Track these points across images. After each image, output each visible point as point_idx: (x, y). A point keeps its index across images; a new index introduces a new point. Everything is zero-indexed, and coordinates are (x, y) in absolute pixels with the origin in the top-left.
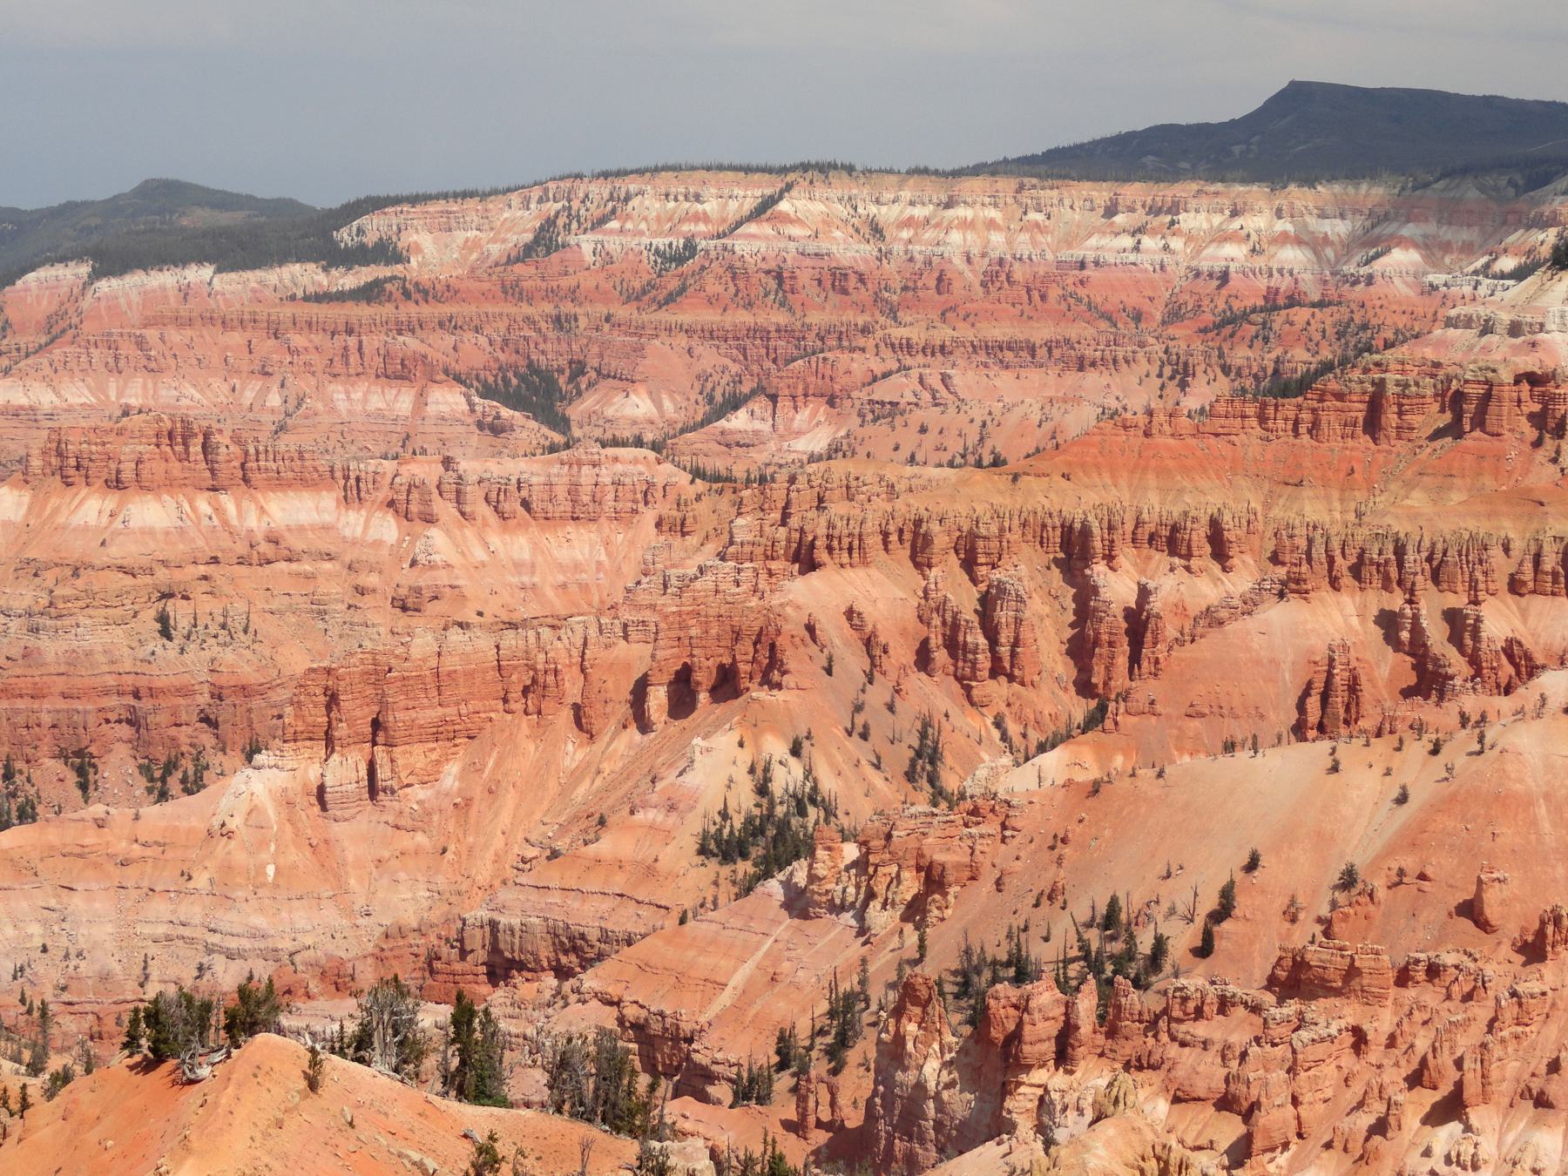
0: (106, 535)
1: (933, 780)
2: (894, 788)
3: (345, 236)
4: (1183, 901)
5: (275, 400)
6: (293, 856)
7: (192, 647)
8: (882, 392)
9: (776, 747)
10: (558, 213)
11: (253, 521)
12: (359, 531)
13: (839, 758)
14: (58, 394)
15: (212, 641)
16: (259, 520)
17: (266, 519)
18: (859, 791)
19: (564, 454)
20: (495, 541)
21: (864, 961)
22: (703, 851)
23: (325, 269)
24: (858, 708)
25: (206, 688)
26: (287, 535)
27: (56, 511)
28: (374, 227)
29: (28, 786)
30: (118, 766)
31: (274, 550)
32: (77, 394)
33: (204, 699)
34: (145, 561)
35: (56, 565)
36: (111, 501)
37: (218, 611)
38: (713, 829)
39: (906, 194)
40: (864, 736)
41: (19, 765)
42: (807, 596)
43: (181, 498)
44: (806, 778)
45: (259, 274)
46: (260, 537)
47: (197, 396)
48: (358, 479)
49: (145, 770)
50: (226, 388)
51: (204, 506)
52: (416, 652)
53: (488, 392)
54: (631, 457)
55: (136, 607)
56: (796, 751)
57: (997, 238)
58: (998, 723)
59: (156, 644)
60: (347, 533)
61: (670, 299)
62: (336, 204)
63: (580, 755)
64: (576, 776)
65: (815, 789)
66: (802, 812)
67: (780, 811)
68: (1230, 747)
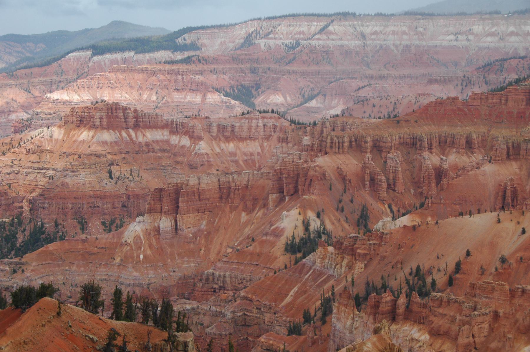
0: (90, 144)
1: (365, 226)
2: (352, 228)
6: (149, 252)
7: (120, 182)
9: (311, 215)
11: (140, 139)
12: (177, 142)
13: (333, 218)
15: (126, 180)
16: (143, 139)
17: (145, 138)
18: (340, 229)
19: (247, 116)
20: (223, 145)
21: (333, 287)
22: (286, 250)
24: (340, 201)
25: (124, 196)
26: (152, 143)
27: (74, 136)
29: (63, 229)
35: (73, 154)
36: (92, 133)
37: (128, 169)
38: (289, 242)
40: (342, 210)
41: (60, 222)
42: (324, 162)
43: (116, 131)
44: (321, 225)
46: (143, 144)
48: (177, 125)
49: (103, 223)
51: (124, 134)
52: (191, 183)
54: (269, 117)
55: (101, 168)
56: (318, 216)
58: (390, 207)
59: (107, 181)
60: (173, 142)
63: (246, 218)
65: (324, 229)
66: (320, 237)
67: (312, 236)
68: (461, 214)
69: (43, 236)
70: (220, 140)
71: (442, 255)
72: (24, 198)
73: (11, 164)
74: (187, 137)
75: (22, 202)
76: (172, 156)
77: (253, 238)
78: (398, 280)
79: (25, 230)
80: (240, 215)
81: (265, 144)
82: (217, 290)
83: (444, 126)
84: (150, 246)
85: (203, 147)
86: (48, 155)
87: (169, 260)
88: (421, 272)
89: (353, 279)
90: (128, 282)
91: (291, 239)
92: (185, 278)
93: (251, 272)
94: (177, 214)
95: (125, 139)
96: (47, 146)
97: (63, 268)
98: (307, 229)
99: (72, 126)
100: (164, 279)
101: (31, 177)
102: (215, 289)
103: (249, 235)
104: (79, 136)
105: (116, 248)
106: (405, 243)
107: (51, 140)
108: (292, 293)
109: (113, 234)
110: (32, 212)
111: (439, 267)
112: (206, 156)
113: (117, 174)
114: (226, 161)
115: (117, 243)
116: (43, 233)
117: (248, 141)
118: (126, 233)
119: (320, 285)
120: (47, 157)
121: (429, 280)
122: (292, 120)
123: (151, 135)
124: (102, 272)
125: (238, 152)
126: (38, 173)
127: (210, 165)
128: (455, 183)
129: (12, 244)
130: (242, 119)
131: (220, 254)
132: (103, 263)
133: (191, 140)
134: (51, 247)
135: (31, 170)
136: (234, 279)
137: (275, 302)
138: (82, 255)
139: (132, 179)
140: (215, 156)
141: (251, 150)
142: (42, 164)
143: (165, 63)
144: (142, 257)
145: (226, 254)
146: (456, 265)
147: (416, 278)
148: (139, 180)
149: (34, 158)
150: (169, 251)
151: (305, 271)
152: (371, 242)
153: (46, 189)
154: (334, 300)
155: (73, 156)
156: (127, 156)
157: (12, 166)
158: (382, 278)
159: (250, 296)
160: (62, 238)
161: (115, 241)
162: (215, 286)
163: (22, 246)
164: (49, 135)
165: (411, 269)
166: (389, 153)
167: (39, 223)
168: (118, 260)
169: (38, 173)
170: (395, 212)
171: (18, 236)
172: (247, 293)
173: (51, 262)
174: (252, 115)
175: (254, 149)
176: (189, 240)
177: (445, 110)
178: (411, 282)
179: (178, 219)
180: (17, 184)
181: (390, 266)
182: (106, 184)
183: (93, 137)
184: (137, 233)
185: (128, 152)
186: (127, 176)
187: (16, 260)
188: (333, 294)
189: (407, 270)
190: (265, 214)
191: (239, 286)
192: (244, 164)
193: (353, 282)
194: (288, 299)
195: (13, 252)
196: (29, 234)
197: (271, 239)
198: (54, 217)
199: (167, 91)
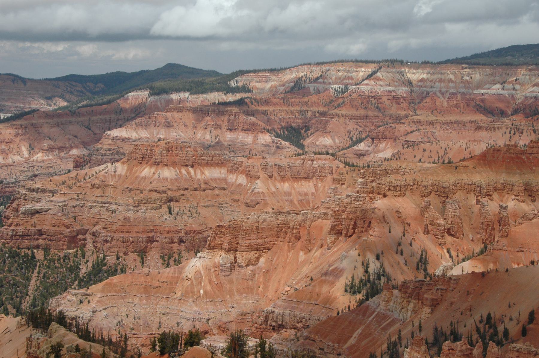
0: (151, 180)
1: (425, 270)
2: (411, 272)
3: (232, 83)
4: (515, 315)
5: (208, 137)
6: (209, 288)
7: (179, 218)
8: (410, 138)
10: (302, 77)
11: (199, 176)
12: (234, 180)
13: (392, 260)
14: (137, 134)
15: (184, 216)
17: (203, 176)
19: (302, 157)
20: (278, 185)
21: (400, 331)
22: (346, 291)
23: (225, 94)
26: (211, 181)
28: (241, 81)
29: (124, 261)
30: (153, 256)
31: (206, 187)
32: (144, 134)
33: (182, 234)
34: (164, 189)
36: (153, 170)
37: (187, 205)
38: (349, 283)
39: (420, 71)
40: (402, 254)
41: (121, 254)
44: (381, 267)
45: (205, 96)
47: (183, 135)
49: (162, 257)
50: (192, 133)
53: (278, 136)
54: (323, 158)
55: (161, 204)
56: (378, 258)
57: (451, 85)
60: (230, 181)
61: (339, 106)
62: (229, 72)
63: (304, 257)
64: (304, 263)
65: (384, 271)
66: (380, 279)
67: (372, 278)
69: (105, 268)
70: (275, 179)
71: (514, 304)
72: (87, 230)
73: (77, 197)
74: (244, 176)
75: (85, 234)
76: (229, 194)
77: (312, 278)
78: (468, 327)
79: (88, 261)
80: (298, 254)
81: (319, 185)
82: (276, 328)
83: (502, 173)
84: (210, 282)
85: (259, 185)
86: (112, 190)
87: (228, 296)
88: (493, 321)
89: (420, 324)
90: (188, 316)
91: (351, 280)
92: (244, 314)
93: (310, 312)
94: (237, 250)
95: (184, 176)
96: (110, 181)
97: (127, 300)
98: (366, 271)
99: (135, 162)
100: (223, 314)
101: (95, 210)
102: (274, 326)
103: (307, 274)
104: (141, 172)
105: (177, 283)
106: (474, 290)
107: (115, 176)
108: (355, 335)
109: (174, 268)
110: (95, 244)
111: (511, 317)
112: (261, 195)
113: (176, 210)
114: (282, 200)
115: (178, 277)
116: (105, 265)
117: (303, 181)
118: (187, 268)
119: (385, 329)
120: (110, 192)
121: (501, 328)
122: (347, 163)
123: (210, 173)
124: (163, 305)
125: (293, 191)
126: (102, 207)
127: (266, 204)
128: (518, 230)
129: (75, 274)
130: (297, 159)
131: (278, 292)
132: (165, 297)
133: (247, 178)
134: (115, 279)
135: (95, 204)
136: (293, 318)
137: (339, 343)
138: (145, 288)
139: (190, 215)
140: (271, 195)
141: (305, 190)
142: (106, 198)
143: (219, 104)
144: (202, 292)
145: (284, 292)
146: (529, 315)
147: (487, 326)
148: (197, 216)
149: (98, 192)
150: (228, 287)
151: (368, 314)
152: (438, 287)
153: (109, 223)
154: (401, 344)
155: (135, 191)
156: (186, 192)
157: (77, 200)
158: (451, 324)
159: (313, 336)
160: (123, 271)
161: (176, 275)
162: (274, 324)
163: (85, 277)
164: (113, 170)
165: (481, 317)
166: (447, 197)
167: (102, 256)
168: (179, 294)
169: (102, 207)
170: (454, 257)
171: (81, 267)
172: (310, 332)
173: (115, 294)
174: (307, 157)
175: (309, 189)
176: (248, 277)
177: (503, 157)
178: (482, 330)
179: (238, 256)
180: (81, 217)
181: (459, 313)
182: (166, 219)
183: (154, 173)
184: (198, 269)
185: (186, 189)
186: (185, 212)
187: (83, 291)
188: (400, 338)
189: (477, 317)
190: (322, 254)
191: (298, 325)
192: (299, 203)
193: (420, 327)
194: (352, 341)
195: (76, 283)
196: (91, 265)
197: (331, 279)
198: (117, 249)
199: (220, 131)
